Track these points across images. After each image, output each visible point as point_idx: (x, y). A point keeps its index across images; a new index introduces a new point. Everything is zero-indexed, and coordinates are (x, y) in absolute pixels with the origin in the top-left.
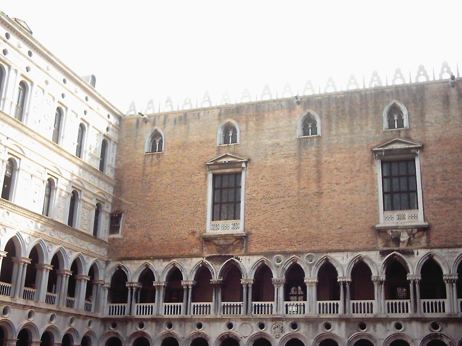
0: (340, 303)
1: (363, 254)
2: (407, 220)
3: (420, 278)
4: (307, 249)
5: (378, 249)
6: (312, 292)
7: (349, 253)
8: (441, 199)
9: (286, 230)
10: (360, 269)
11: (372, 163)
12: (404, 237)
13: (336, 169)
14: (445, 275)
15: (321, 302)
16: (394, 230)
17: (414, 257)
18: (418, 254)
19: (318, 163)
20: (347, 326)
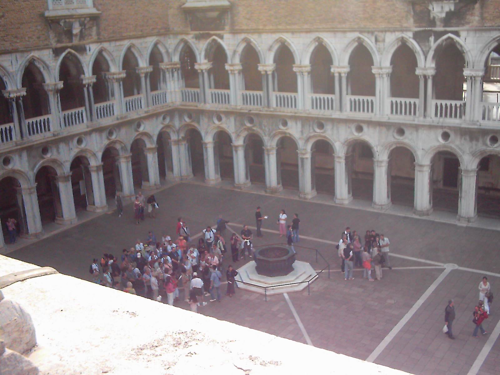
1: (36, 54)
5: (50, 46)
7: (19, 55)
12: (76, 30)
14: (114, 74)
16: (67, 20)
17: (87, 54)
20: (29, 156)
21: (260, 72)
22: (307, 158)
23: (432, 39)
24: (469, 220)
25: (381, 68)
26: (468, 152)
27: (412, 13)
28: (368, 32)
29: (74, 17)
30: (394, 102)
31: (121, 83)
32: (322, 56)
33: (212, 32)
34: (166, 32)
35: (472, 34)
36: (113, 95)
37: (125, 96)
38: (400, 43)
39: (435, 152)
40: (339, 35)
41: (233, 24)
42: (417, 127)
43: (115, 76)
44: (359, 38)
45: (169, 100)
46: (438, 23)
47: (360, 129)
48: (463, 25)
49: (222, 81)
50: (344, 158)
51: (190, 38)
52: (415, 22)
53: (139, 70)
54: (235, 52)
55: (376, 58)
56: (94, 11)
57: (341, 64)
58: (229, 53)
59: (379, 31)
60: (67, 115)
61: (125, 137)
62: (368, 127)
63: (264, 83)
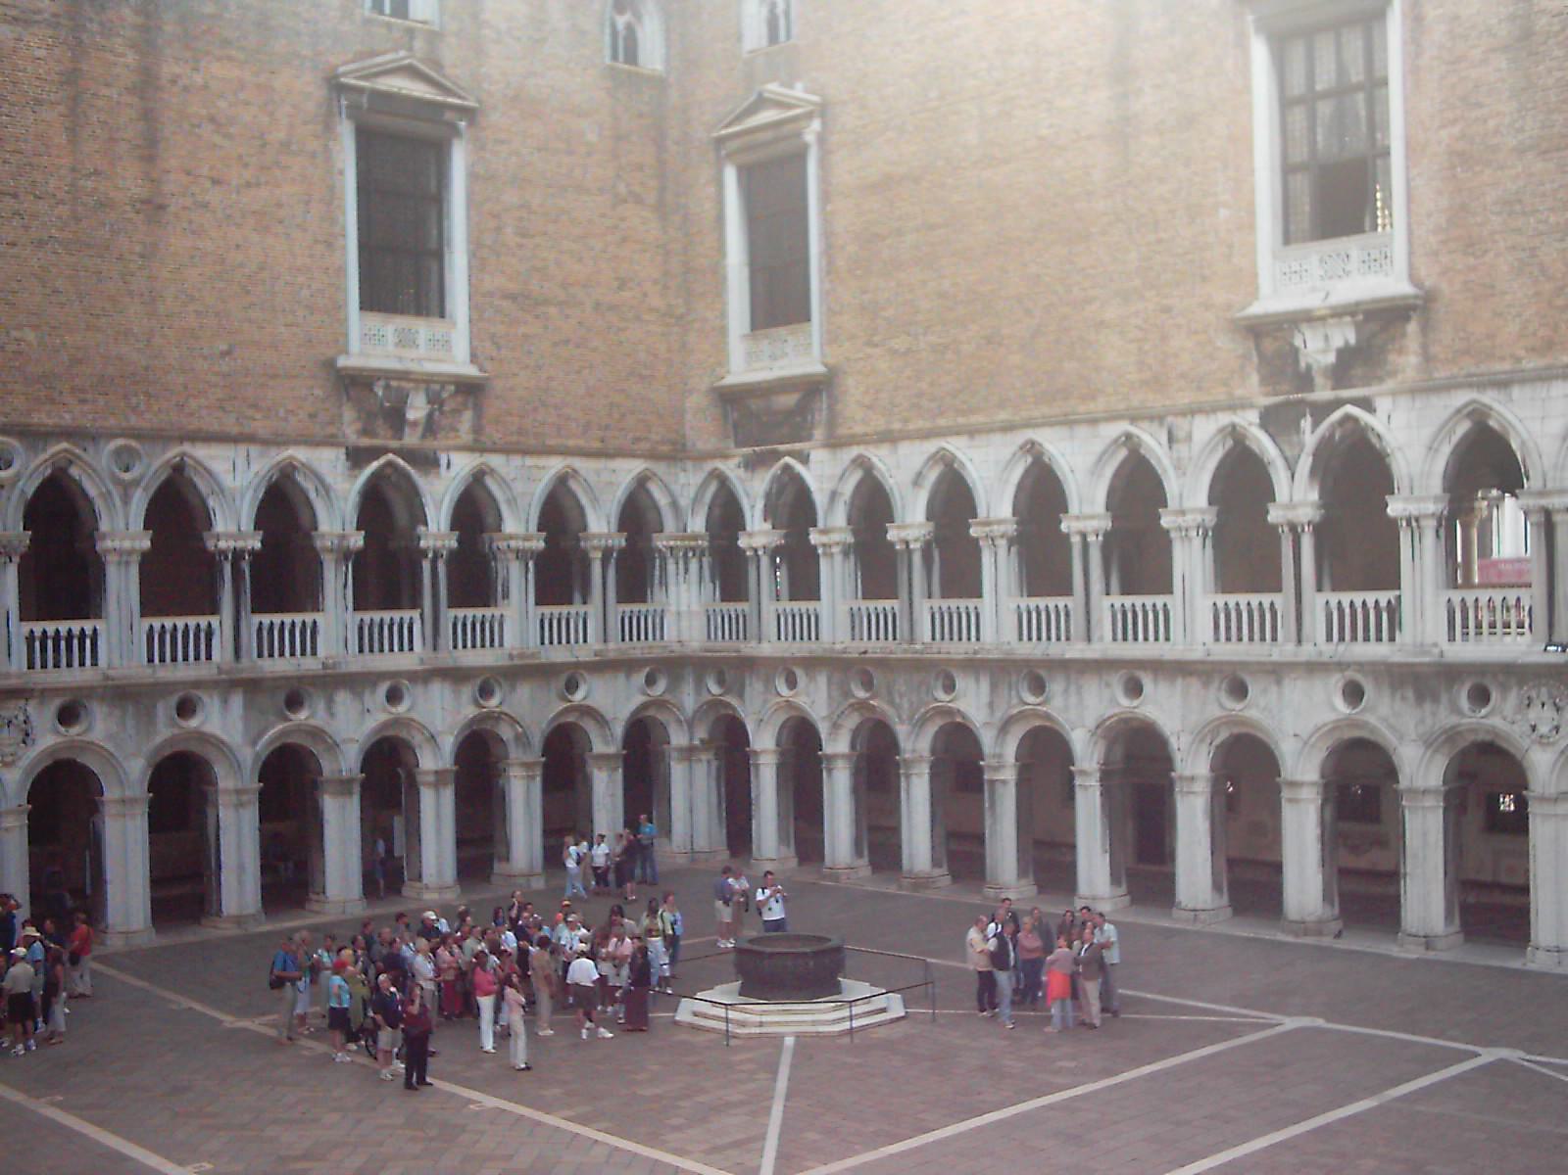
1: (300, 454)
2: (422, 351)
3: (454, 544)
4: (112, 422)
5: (342, 440)
6: (122, 586)
7: (254, 450)
8: (512, 297)
9: (30, 336)
10: (282, 506)
11: (329, 127)
12: (417, 410)
13: (212, 119)
14: (511, 537)
15: (157, 623)
16: (394, 383)
17: (438, 473)
18: (449, 465)
19: (147, 83)
20: (248, 706)
21: (892, 545)
22: (1004, 782)
23: (1306, 423)
24: (1428, 942)
25: (1183, 513)
26: (1414, 737)
27: (1255, 359)
28: (1151, 418)
29: (412, 377)
30: (1221, 605)
31: (531, 564)
32: (1042, 493)
33: (782, 448)
34: (677, 453)
35: (1404, 401)
36: (506, 595)
38: (1230, 443)
39: (1329, 742)
40: (1082, 431)
41: (832, 424)
42: (1276, 672)
43: (513, 544)
44: (1129, 436)
45: (670, 632)
46: (1319, 380)
47: (1135, 689)
48: (1381, 380)
49: (801, 572)
51: (731, 468)
52: (1263, 381)
53: (587, 539)
54: (834, 495)
55: (1172, 486)
56: (472, 371)
57: (1087, 510)
58: (820, 499)
59: (1176, 415)
61: (530, 711)
62: (1155, 681)
63: (903, 576)
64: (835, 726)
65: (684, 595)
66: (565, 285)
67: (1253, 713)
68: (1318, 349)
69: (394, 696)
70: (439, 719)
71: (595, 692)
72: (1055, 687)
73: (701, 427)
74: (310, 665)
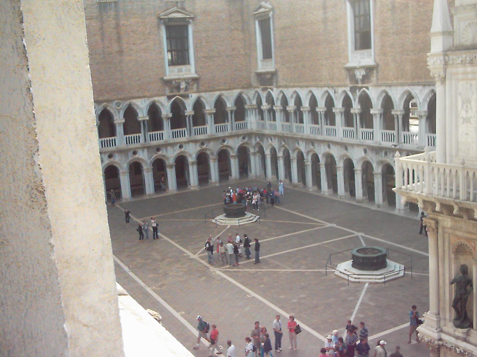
0: (141, 135)
1: (156, 99)
2: (184, 73)
4: (115, 97)
7: (146, 99)
10: (154, 110)
12: (183, 85)
14: (208, 110)
15: (128, 136)
16: (177, 81)
17: (189, 99)
18: (191, 97)
20: (148, 151)
23: (357, 91)
24: (379, 206)
27: (348, 76)
29: (181, 79)
31: (213, 116)
32: (313, 102)
34: (249, 86)
37: (215, 123)
40: (320, 89)
41: (277, 82)
46: (359, 82)
47: (329, 147)
50: (324, 165)
51: (259, 90)
53: (227, 108)
54: (277, 99)
56: (196, 76)
57: (321, 107)
58: (275, 99)
60: (174, 131)
61: (213, 148)
62: (333, 145)
64: (279, 150)
65: (252, 119)
66: (218, 52)
67: (349, 154)
68: (359, 74)
69: (181, 147)
70: (192, 152)
71: (230, 142)
72: (316, 145)
73: (254, 81)
74: (161, 142)
